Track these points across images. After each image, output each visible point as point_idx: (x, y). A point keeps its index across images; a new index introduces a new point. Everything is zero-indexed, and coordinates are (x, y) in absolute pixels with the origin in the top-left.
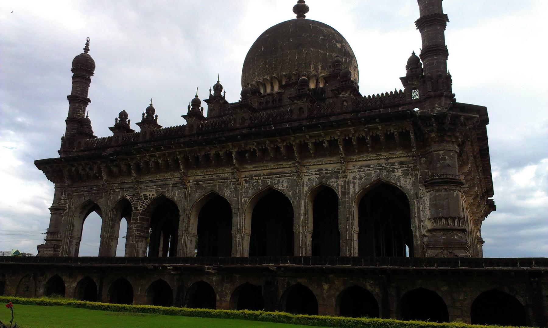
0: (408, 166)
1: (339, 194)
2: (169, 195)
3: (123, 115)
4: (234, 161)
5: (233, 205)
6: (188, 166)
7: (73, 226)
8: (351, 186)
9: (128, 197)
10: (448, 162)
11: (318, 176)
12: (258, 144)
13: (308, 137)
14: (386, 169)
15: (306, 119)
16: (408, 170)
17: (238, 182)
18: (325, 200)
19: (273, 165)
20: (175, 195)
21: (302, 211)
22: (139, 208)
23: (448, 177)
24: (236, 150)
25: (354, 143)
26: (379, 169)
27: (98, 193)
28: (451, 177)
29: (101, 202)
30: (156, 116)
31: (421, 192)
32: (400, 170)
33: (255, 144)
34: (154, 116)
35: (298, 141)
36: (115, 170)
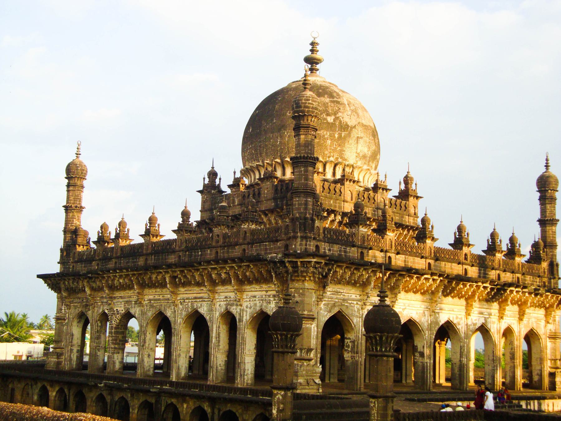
5: (172, 325)
10: (297, 299)
22: (113, 322)
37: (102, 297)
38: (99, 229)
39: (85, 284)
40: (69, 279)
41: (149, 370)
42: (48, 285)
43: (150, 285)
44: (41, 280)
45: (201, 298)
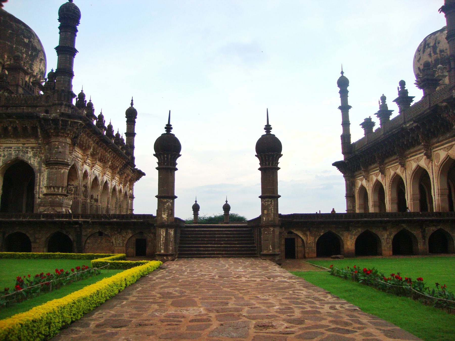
0: (37, 150)
10: (61, 150)
14: (22, 151)
16: (37, 153)
26: (17, 151)
32: (32, 152)
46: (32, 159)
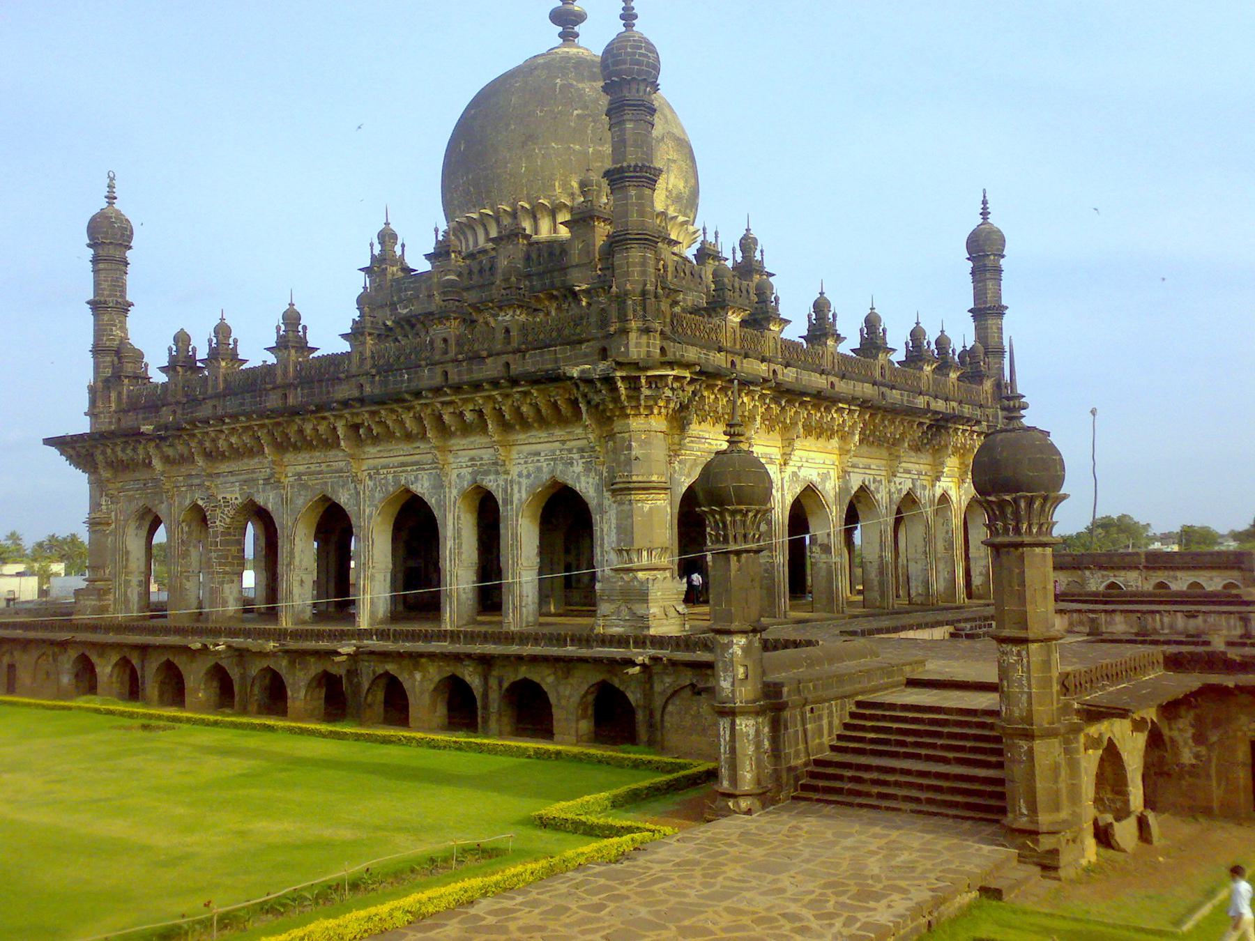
1: (500, 502)
2: (260, 500)
3: (182, 339)
4: (342, 443)
5: (354, 521)
6: (283, 446)
7: (127, 553)
8: (516, 488)
9: (200, 503)
11: (470, 470)
12: (373, 413)
13: (439, 406)
15: (453, 361)
17: (356, 480)
18: (487, 511)
19: (407, 447)
20: (267, 499)
21: (449, 533)
23: (634, 478)
24: (343, 422)
25: (507, 417)
27: (156, 494)
28: (640, 479)
29: (162, 510)
30: (235, 341)
31: (606, 503)
33: (367, 415)
34: (231, 341)
35: (429, 411)
36: (170, 452)
37: (190, 476)
38: (171, 343)
39: (152, 451)
40: (116, 444)
41: (303, 612)
42: (69, 458)
43: (299, 444)
44: (54, 451)
45: (413, 464)
46: (583, 479)
